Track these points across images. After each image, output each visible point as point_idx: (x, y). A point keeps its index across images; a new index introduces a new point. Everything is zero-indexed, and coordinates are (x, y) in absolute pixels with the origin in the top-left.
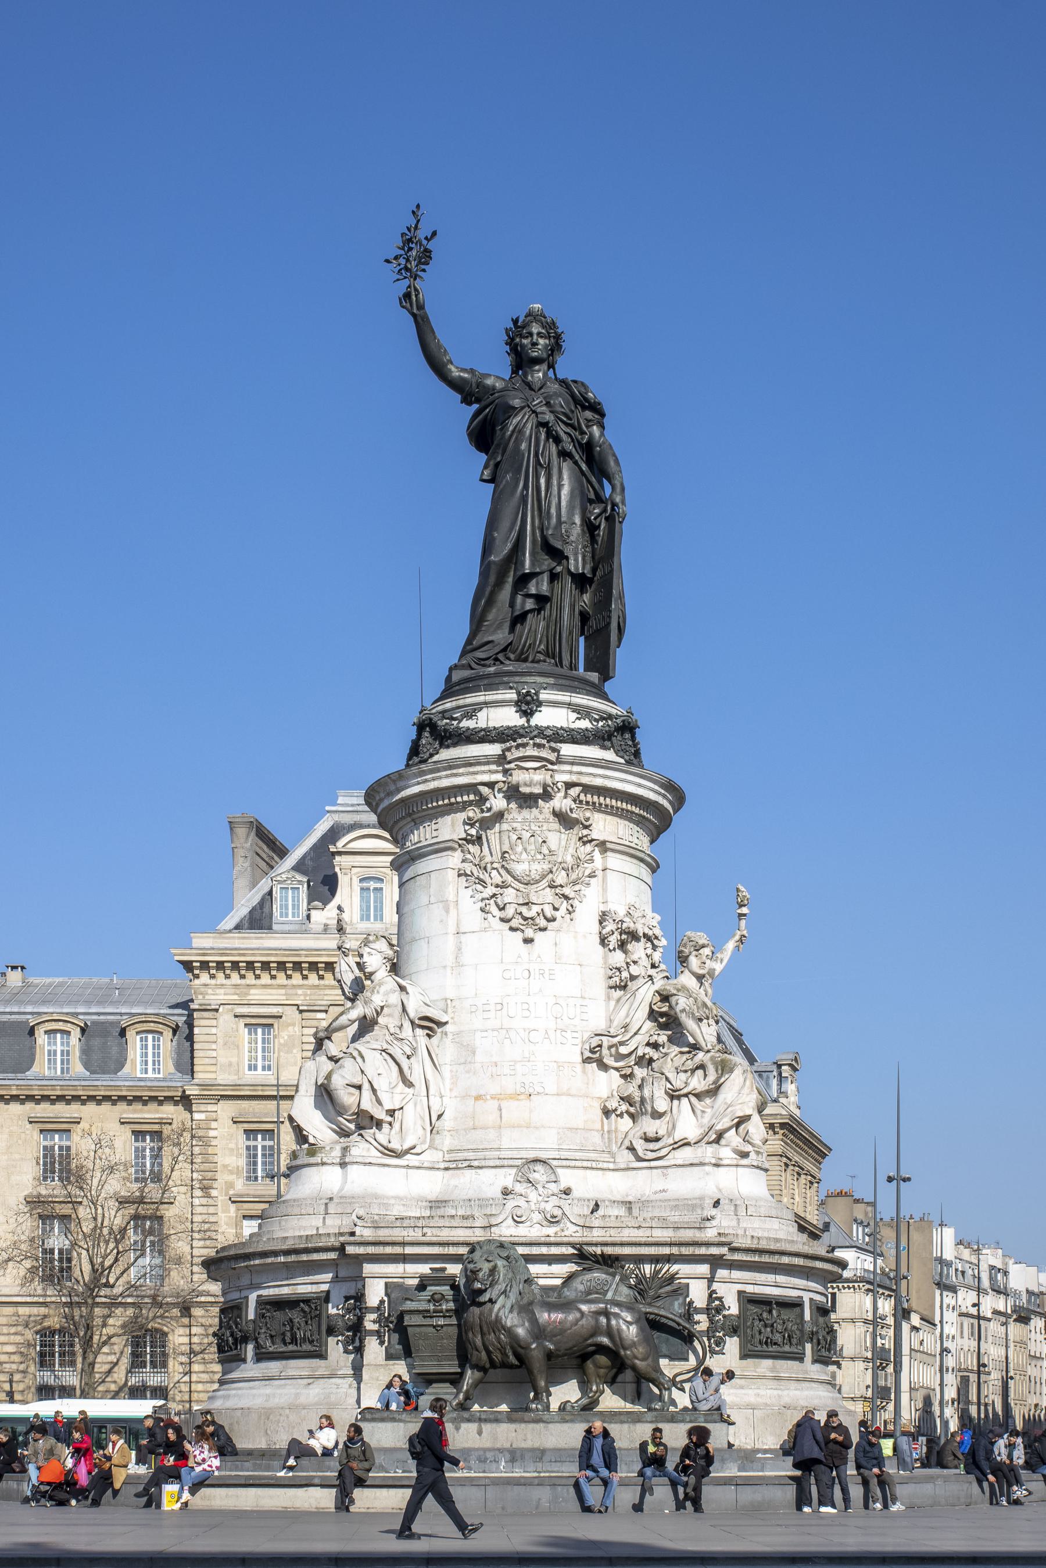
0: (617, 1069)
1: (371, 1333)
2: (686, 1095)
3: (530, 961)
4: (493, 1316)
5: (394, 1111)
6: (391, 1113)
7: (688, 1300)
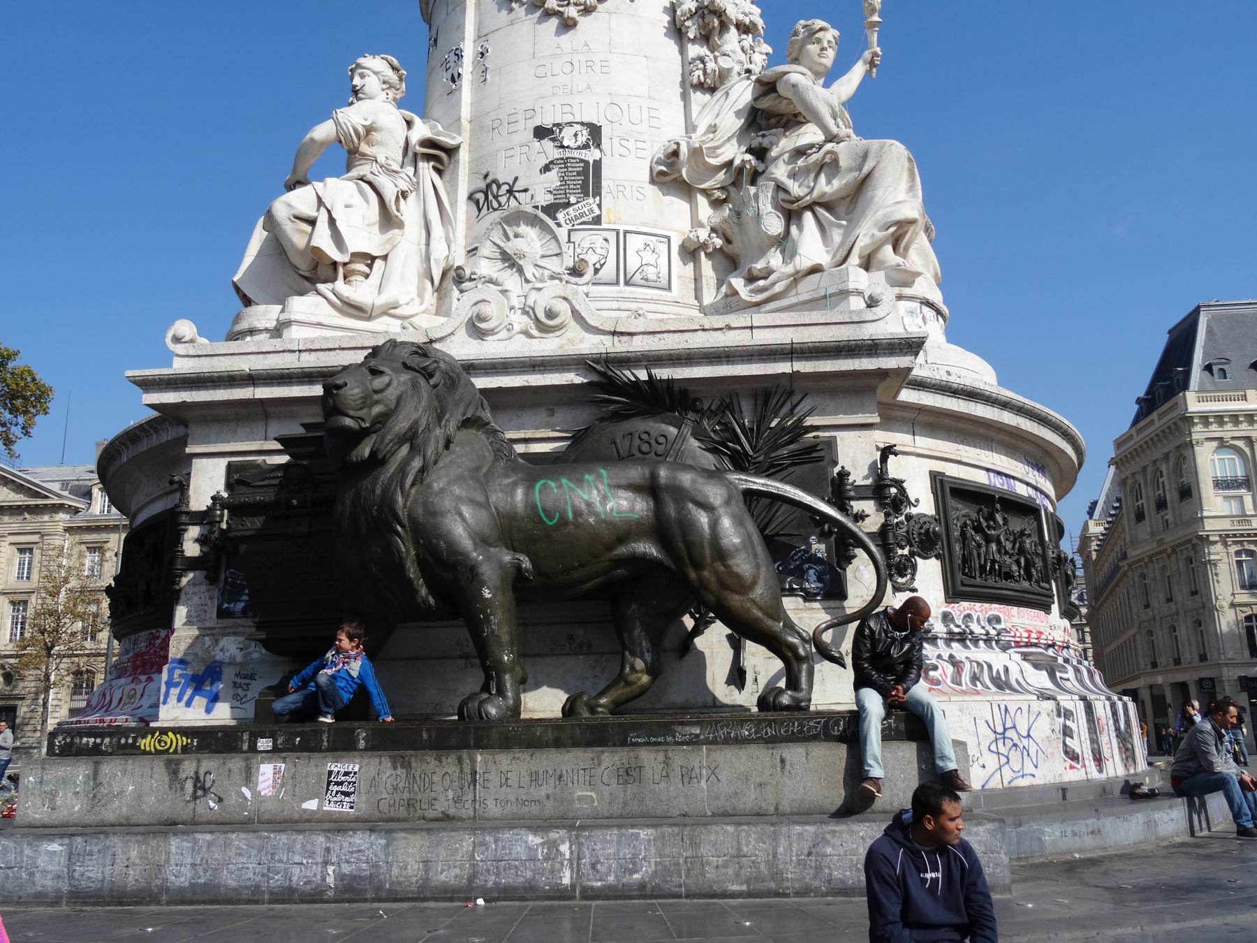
0: (705, 192)
1: (193, 564)
2: (810, 207)
3: (573, 52)
4: (378, 491)
5: (373, 258)
6: (370, 259)
7: (837, 470)
